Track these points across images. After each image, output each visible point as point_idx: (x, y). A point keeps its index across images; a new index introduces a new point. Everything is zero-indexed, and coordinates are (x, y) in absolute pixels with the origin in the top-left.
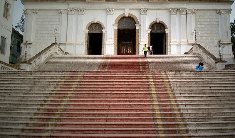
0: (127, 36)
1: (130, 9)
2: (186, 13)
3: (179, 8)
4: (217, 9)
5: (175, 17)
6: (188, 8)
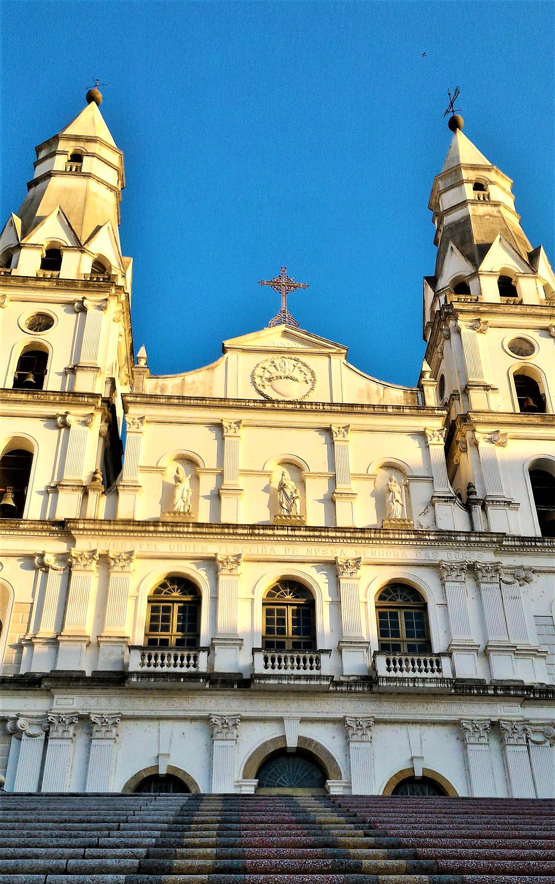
1: (303, 720)
2: (527, 739)
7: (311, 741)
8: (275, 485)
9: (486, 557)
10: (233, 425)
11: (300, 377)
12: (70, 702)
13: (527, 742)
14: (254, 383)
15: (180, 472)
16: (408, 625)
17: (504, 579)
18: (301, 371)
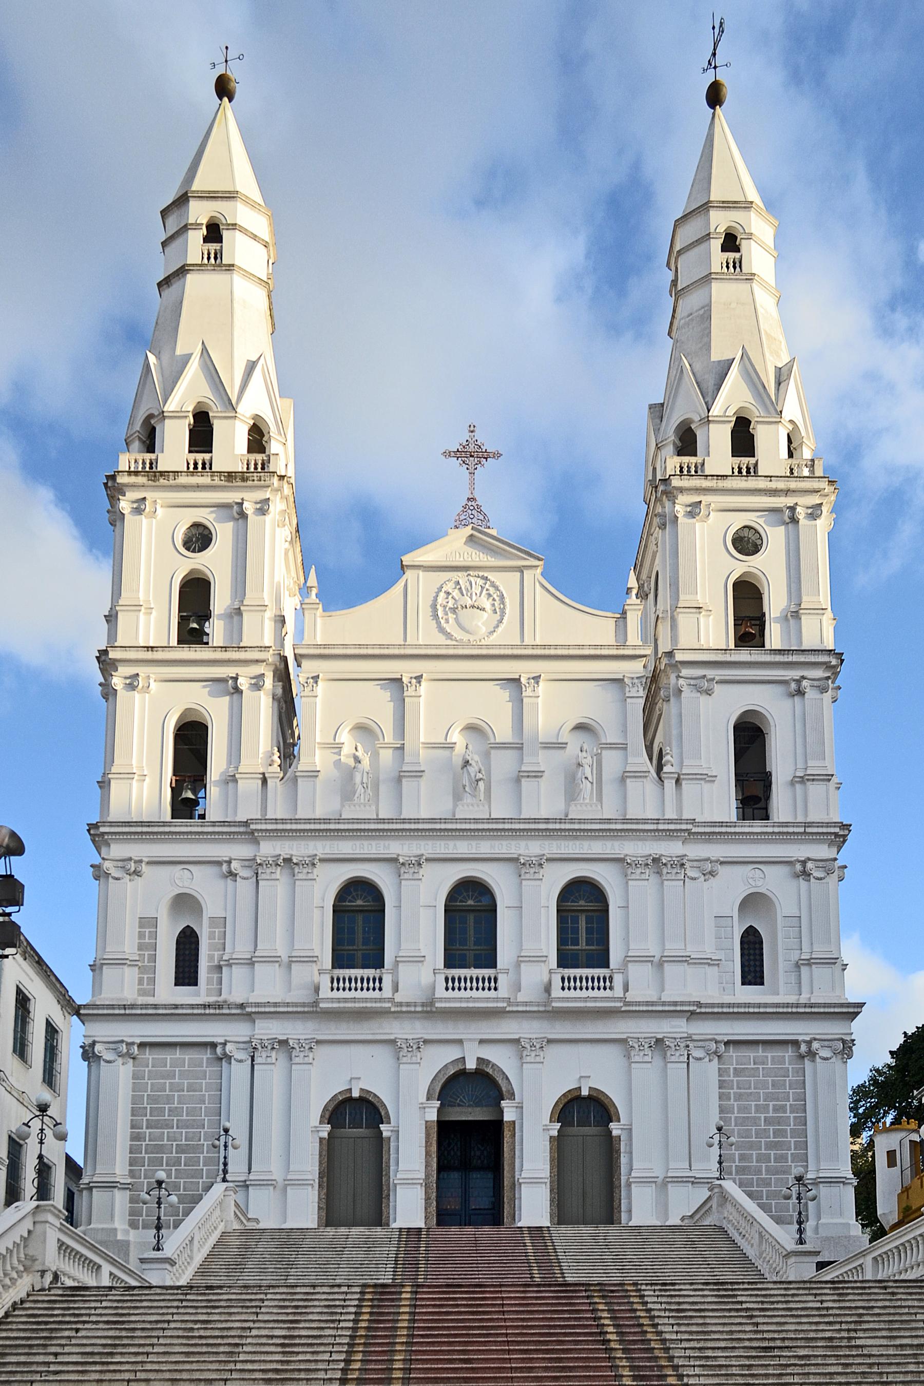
0: (471, 1146)
1: (482, 1041)
2: (688, 1055)
3: (660, 1036)
4: (800, 1038)
5: (647, 1071)
6: (694, 1037)
7: (488, 1062)
8: (458, 761)
9: (671, 849)
10: (414, 681)
11: (487, 604)
12: (268, 1029)
13: (688, 1059)
14: (435, 616)
15: (359, 748)
16: (589, 931)
17: (691, 873)
18: (489, 595)
